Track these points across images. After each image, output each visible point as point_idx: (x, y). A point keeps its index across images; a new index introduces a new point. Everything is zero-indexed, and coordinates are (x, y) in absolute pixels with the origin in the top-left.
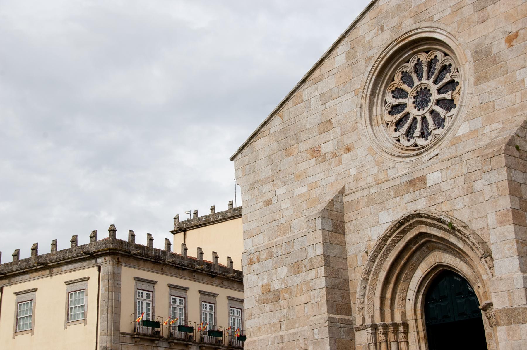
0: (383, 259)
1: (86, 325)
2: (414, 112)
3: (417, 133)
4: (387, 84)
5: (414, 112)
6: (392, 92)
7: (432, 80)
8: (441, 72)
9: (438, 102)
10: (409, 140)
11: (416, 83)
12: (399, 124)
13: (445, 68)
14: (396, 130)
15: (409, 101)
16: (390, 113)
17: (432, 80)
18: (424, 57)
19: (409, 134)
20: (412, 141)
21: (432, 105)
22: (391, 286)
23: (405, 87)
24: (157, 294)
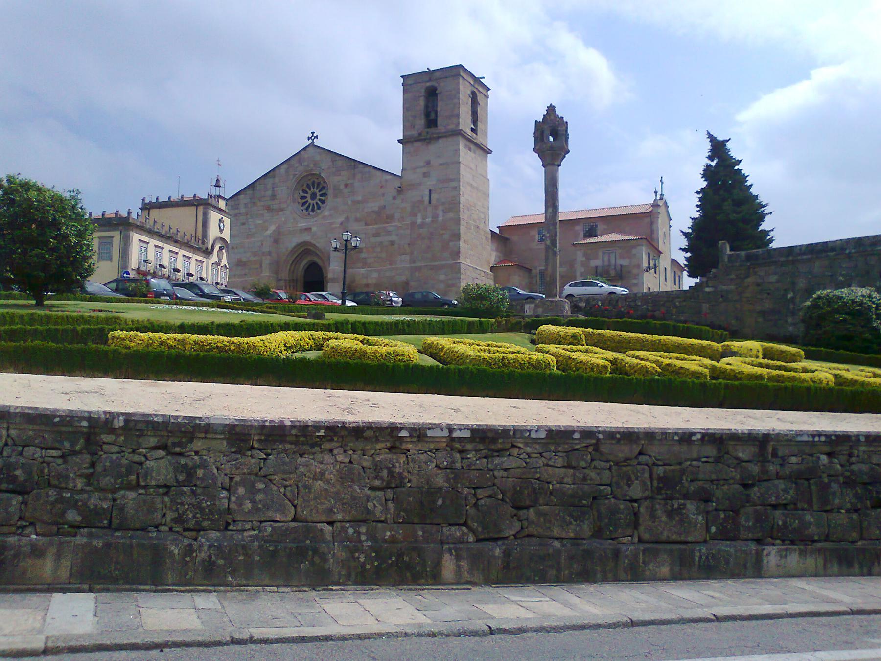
1: (111, 262)
2: (310, 201)
3: (310, 209)
5: (310, 201)
12: (303, 204)
13: (323, 188)
15: (308, 196)
17: (319, 189)
19: (307, 209)
20: (308, 212)
21: (317, 200)
24: (149, 249)
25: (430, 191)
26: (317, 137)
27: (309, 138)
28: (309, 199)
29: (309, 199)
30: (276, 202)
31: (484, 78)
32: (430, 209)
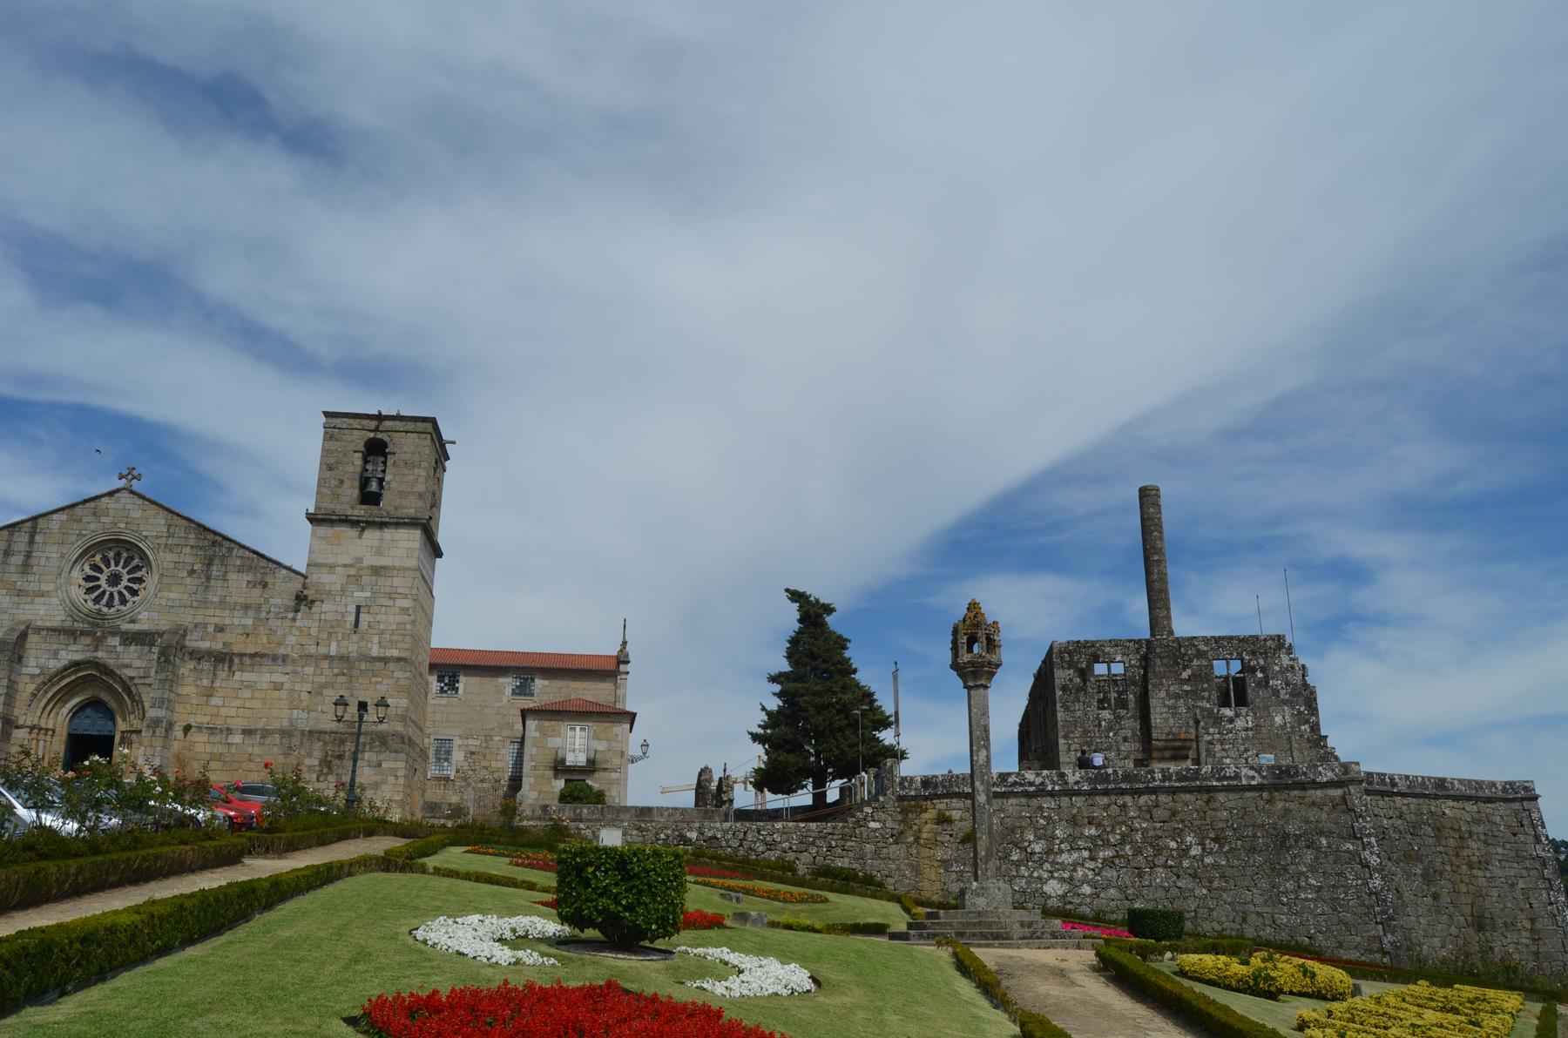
0: (53, 685)
3: (104, 601)
4: (89, 557)
6: (90, 565)
7: (126, 570)
8: (134, 568)
9: (126, 588)
11: (113, 567)
13: (137, 568)
14: (85, 593)
15: (103, 578)
16: (84, 579)
17: (126, 570)
19: (97, 601)
20: (97, 607)
21: (121, 587)
22: (53, 702)
25: (358, 608)
26: (138, 478)
28: (103, 582)
29: (103, 582)
30: (31, 577)
31: (454, 443)
32: (354, 638)
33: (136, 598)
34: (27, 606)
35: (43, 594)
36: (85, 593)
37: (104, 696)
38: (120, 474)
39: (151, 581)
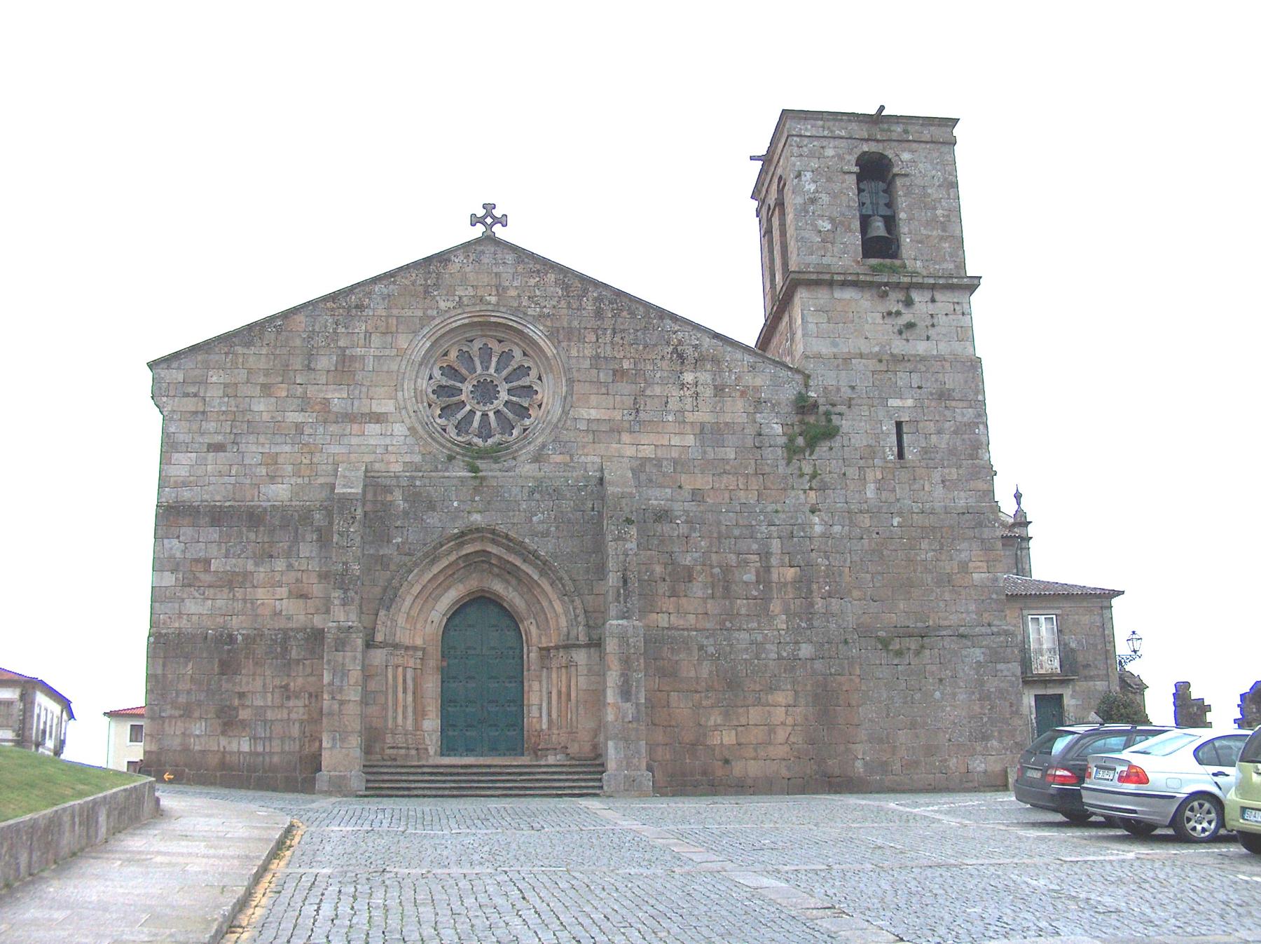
6: (441, 368)
10: (458, 435)
15: (467, 387)
16: (434, 392)
18: (496, 348)
21: (498, 404)
23: (464, 371)
25: (899, 425)
27: (475, 220)
33: (527, 422)
34: (354, 441)
35: (378, 418)
36: (440, 416)
37: (498, 587)
38: (473, 216)
39: (549, 393)
